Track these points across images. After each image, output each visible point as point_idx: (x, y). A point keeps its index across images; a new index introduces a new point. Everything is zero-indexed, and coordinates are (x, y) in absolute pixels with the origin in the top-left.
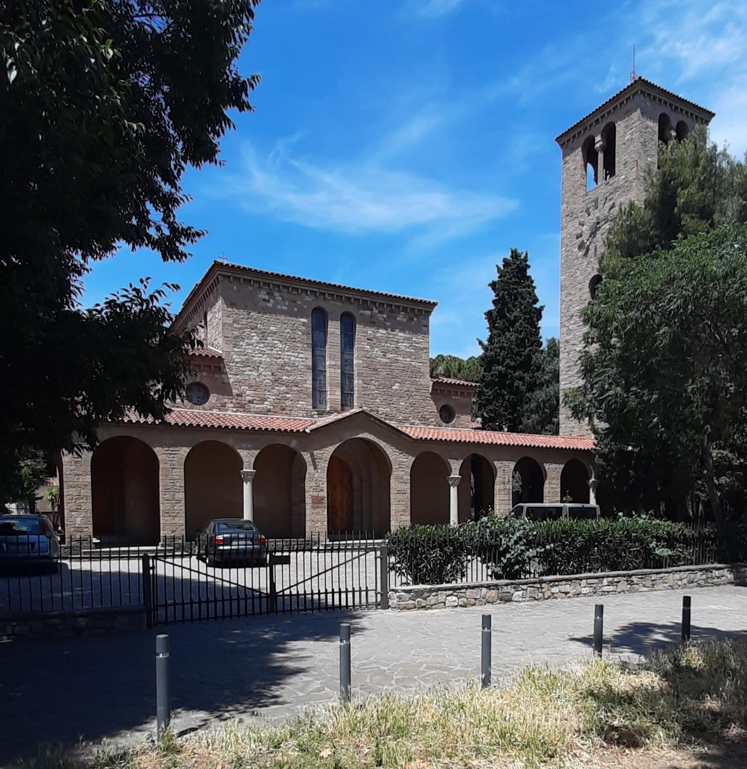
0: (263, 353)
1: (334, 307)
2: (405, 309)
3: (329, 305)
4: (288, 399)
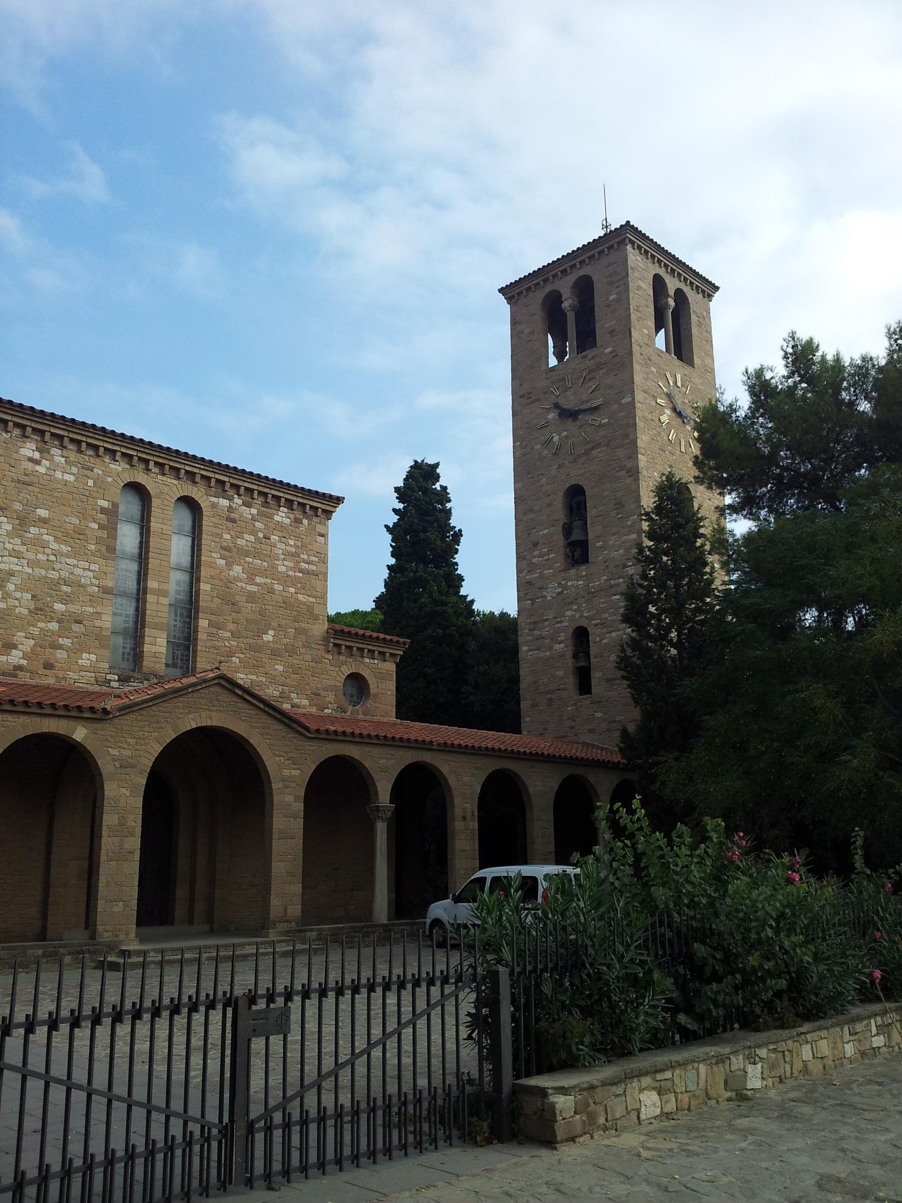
0: (18, 555)
1: (165, 489)
2: (289, 504)
3: (151, 481)
4: (60, 647)
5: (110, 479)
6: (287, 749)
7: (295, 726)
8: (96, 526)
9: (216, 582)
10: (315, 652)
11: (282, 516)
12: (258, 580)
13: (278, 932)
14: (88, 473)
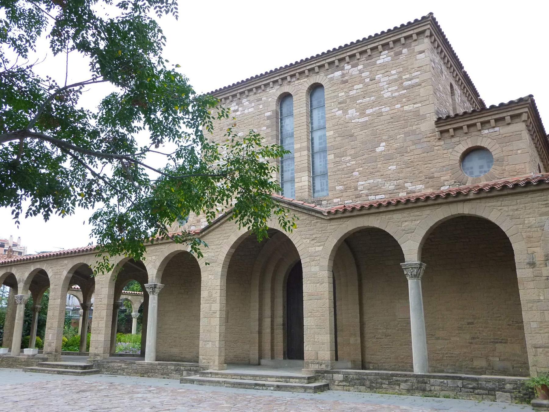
2: (385, 46)
5: (270, 99)
6: (312, 232)
7: (313, 214)
8: (265, 128)
9: (337, 127)
10: (425, 145)
11: (384, 58)
12: (368, 111)
13: (309, 371)
14: (259, 102)
